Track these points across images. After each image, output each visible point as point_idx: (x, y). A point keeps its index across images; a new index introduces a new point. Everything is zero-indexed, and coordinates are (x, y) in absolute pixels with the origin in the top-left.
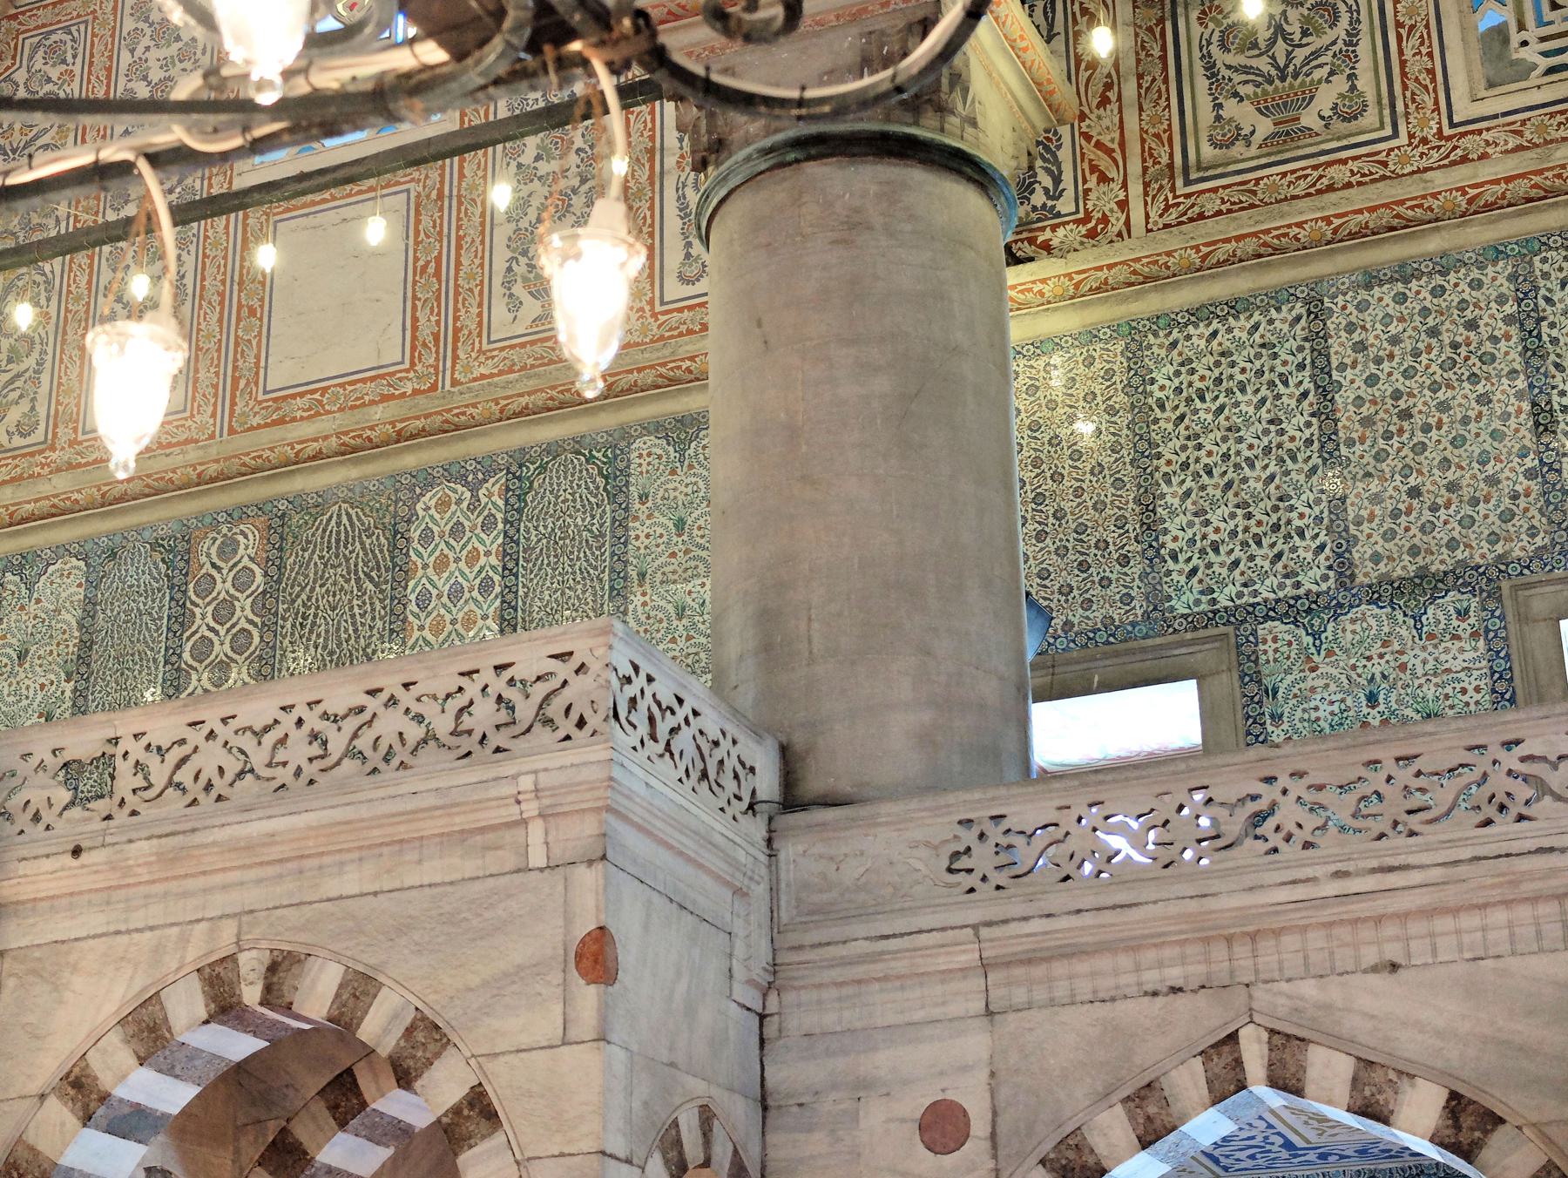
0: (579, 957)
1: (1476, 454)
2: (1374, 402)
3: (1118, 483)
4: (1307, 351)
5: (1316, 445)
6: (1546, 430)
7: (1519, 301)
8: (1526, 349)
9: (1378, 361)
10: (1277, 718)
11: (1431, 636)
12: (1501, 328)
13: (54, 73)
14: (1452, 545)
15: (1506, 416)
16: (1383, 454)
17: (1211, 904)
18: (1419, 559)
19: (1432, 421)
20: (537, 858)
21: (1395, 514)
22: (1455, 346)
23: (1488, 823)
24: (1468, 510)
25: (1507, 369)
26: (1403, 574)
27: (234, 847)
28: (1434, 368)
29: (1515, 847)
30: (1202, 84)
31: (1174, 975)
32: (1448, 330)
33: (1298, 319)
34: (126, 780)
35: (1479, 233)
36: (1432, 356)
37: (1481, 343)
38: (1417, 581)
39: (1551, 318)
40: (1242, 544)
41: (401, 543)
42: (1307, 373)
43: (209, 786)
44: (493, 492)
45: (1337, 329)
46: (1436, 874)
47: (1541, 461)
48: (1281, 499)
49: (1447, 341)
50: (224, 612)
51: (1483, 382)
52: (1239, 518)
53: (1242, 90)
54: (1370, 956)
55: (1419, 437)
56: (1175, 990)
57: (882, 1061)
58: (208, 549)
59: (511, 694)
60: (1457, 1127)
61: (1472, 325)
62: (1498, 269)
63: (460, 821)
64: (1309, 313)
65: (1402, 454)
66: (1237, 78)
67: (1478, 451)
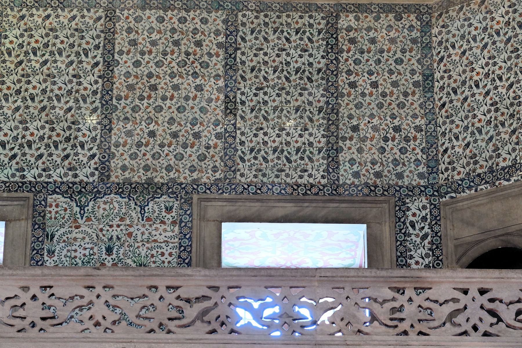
1: (190, 119)
2: (136, 77)
4: (102, 39)
5: (99, 96)
6: (231, 112)
7: (227, 36)
8: (226, 64)
9: (143, 53)
10: (51, 253)
11: (149, 219)
12: (214, 49)
16: (137, 108)
18: (149, 173)
19: (168, 95)
21: (139, 145)
22: (188, 54)
24: (180, 150)
25: (214, 73)
26: (139, 180)
28: (174, 64)
32: (185, 44)
33: (99, 18)
36: (174, 57)
37: (202, 55)
38: (146, 186)
39: (243, 49)
40: (46, 145)
42: (100, 51)
45: (121, 29)
47: (226, 129)
48: (73, 123)
49: (183, 50)
51: (200, 78)
52: (47, 130)
55: (159, 102)
61: (199, 44)
62: (218, 14)
64: (107, 16)
65: (148, 110)
67: (191, 117)
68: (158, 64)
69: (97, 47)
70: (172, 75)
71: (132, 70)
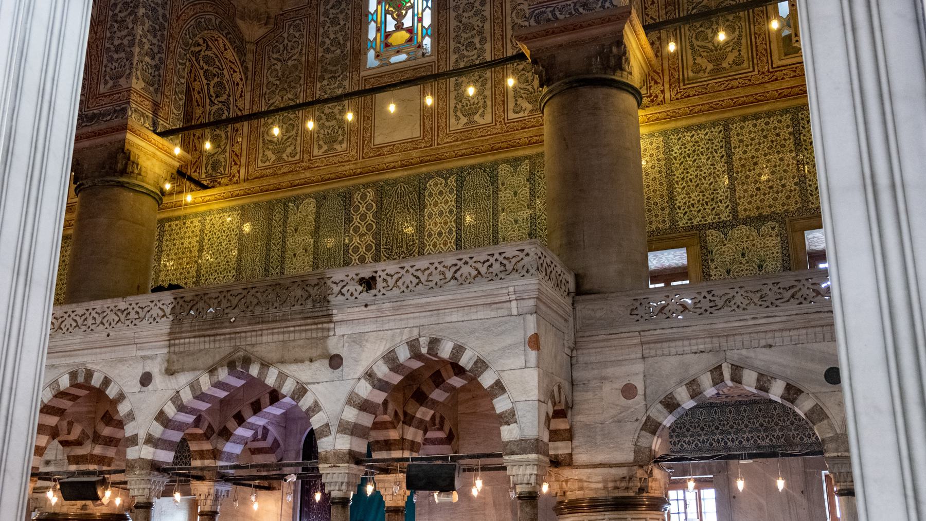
0: (529, 342)
3: (661, 184)
9: (747, 146)
10: (712, 260)
11: (763, 235)
12: (787, 136)
13: (297, 35)
14: (770, 206)
15: (788, 165)
17: (714, 326)
20: (515, 312)
22: (772, 141)
23: (801, 303)
24: (775, 195)
27: (417, 306)
29: (810, 311)
30: (689, 52)
31: (701, 347)
34: (380, 284)
35: (781, 105)
41: (422, 197)
43: (408, 287)
44: (452, 181)
46: (784, 318)
50: (363, 217)
53: (703, 54)
54: (763, 343)
56: (702, 352)
57: (609, 371)
58: (357, 197)
59: (505, 262)
60: (789, 394)
61: (778, 135)
63: (490, 300)
66: (701, 50)
68: (757, 150)
69: (722, 147)
70: (765, 155)
71: (743, 156)
